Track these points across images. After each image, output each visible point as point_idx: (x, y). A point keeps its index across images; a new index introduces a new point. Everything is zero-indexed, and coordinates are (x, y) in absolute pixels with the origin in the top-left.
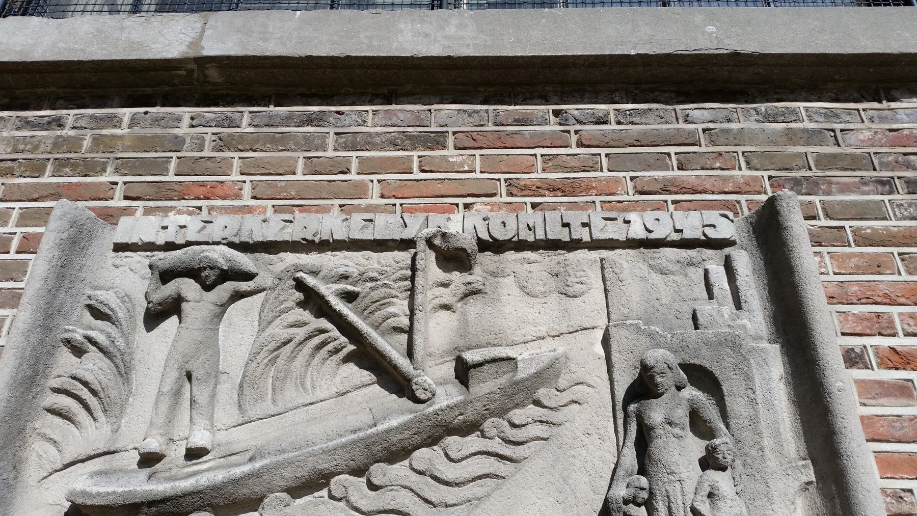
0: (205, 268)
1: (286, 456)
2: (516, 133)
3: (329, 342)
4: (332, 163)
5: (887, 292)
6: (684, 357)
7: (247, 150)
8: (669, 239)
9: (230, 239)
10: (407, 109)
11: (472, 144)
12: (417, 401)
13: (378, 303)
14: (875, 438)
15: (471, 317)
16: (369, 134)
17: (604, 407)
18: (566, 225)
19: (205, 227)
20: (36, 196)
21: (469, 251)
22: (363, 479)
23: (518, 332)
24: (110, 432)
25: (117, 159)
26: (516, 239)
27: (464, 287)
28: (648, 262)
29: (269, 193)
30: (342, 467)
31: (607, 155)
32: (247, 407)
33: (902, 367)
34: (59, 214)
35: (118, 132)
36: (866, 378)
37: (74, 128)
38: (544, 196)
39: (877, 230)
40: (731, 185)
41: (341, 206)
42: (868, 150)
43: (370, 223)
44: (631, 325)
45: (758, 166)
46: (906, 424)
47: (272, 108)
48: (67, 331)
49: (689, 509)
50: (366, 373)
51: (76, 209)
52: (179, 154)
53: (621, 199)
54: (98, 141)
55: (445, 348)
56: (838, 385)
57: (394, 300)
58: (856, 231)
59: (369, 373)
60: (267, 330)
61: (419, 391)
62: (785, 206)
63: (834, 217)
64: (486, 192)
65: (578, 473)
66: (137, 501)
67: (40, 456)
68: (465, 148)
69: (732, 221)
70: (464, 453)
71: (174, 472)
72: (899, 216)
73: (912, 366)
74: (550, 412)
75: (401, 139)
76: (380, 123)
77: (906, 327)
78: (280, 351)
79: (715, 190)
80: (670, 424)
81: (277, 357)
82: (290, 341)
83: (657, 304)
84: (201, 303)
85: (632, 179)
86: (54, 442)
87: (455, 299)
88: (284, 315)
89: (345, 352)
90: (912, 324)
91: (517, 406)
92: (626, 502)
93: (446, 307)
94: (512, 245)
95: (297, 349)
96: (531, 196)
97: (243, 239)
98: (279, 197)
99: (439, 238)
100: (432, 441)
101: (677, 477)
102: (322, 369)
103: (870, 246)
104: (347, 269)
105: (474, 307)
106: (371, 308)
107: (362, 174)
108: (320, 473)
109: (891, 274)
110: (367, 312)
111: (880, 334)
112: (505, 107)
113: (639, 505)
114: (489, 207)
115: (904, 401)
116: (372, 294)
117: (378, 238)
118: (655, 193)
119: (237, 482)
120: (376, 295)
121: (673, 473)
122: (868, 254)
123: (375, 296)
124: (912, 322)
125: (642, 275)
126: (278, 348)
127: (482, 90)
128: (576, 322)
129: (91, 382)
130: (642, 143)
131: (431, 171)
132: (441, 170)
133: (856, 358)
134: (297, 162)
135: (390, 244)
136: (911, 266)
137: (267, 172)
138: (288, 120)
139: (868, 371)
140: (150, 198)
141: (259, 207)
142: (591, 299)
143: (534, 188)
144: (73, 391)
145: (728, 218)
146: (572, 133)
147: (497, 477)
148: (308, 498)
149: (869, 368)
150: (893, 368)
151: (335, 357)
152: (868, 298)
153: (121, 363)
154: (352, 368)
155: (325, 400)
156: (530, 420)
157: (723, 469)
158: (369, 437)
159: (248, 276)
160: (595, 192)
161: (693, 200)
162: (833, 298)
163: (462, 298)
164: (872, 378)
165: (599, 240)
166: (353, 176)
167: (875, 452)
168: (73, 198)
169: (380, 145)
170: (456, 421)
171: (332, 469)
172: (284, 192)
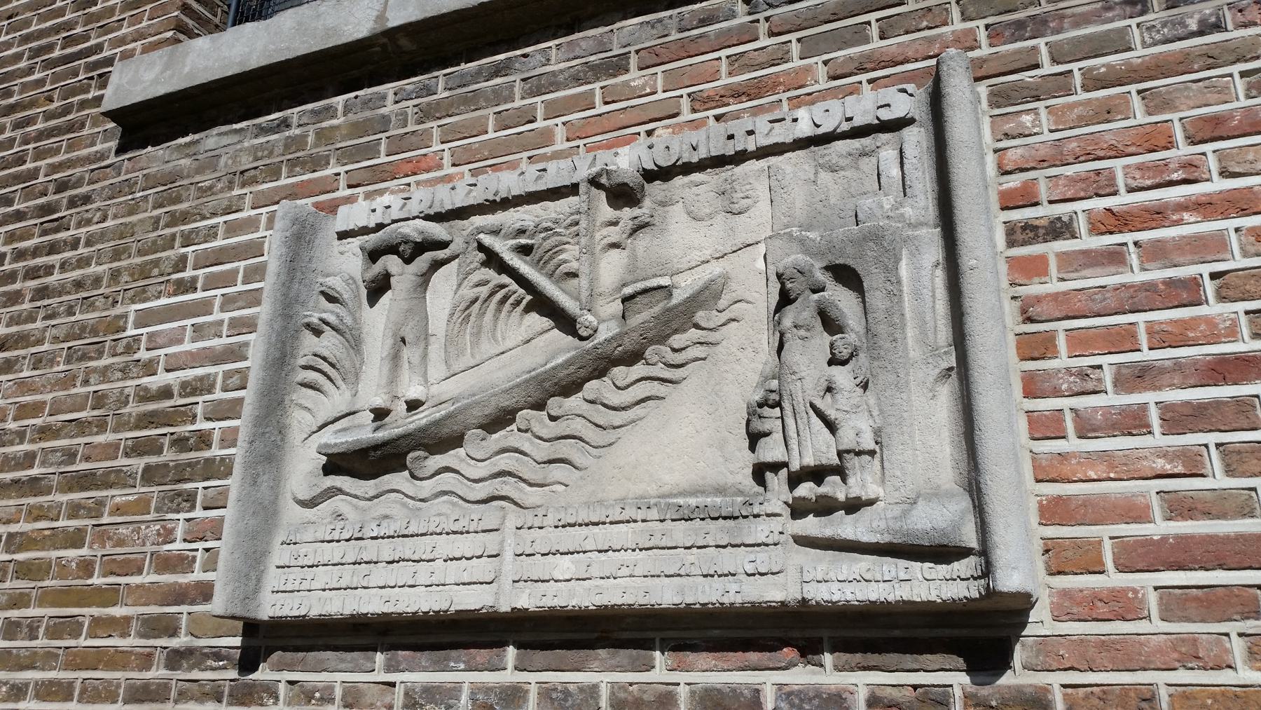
0: (400, 244)
2: (701, 36)
3: (510, 296)
4: (519, 114)
5: (1114, 142)
6: (830, 258)
7: (444, 117)
8: (839, 131)
9: (426, 212)
12: (582, 339)
13: (551, 252)
14: (1070, 314)
15: (640, 252)
16: (553, 73)
17: (760, 320)
18: (731, 137)
19: (405, 204)
21: (631, 185)
23: (684, 260)
25: (338, 149)
27: (632, 223)
28: (818, 161)
31: (799, 40)
33: (1117, 230)
35: (335, 122)
36: (1070, 249)
38: (728, 105)
39: (1113, 66)
40: (938, 46)
41: (530, 158)
44: (784, 234)
45: (974, 15)
47: (463, 66)
49: (808, 405)
50: (545, 319)
51: (296, 207)
52: (387, 134)
53: (810, 91)
54: (320, 134)
56: (970, 263)
57: (566, 246)
58: (1085, 73)
62: (945, 69)
63: (1061, 60)
65: (731, 386)
69: (911, 95)
70: (629, 380)
71: (400, 422)
72: (1149, 41)
73: (1130, 227)
74: (709, 332)
75: (583, 71)
77: (1130, 181)
78: (471, 309)
79: (918, 56)
80: (795, 327)
81: (469, 315)
82: (476, 300)
83: (819, 206)
85: (825, 63)
87: (625, 236)
89: (524, 302)
90: (1137, 177)
91: (676, 331)
92: (760, 405)
93: (615, 245)
94: (679, 170)
95: (484, 306)
96: (714, 108)
99: (605, 176)
100: (600, 373)
101: (798, 376)
103: (1103, 88)
104: (523, 223)
105: (643, 241)
106: (546, 258)
108: (505, 410)
109: (1123, 119)
110: (542, 262)
112: (690, 7)
113: (772, 407)
114: (670, 130)
115: (1113, 269)
118: (850, 75)
119: (437, 423)
121: (794, 373)
122: (1097, 99)
124: (1138, 174)
125: (806, 178)
126: (468, 308)
128: (744, 238)
130: (839, 16)
131: (614, 102)
133: (1062, 228)
134: (488, 119)
137: (462, 136)
138: (477, 76)
139: (1076, 240)
141: (457, 174)
142: (757, 213)
143: (717, 98)
145: (907, 92)
146: (762, 20)
147: (658, 398)
149: (1077, 238)
150: (1106, 232)
151: (518, 309)
152: (1089, 154)
156: (689, 343)
157: (844, 363)
159: (443, 245)
160: (782, 88)
161: (891, 75)
162: (1044, 161)
163: (631, 235)
164: (1077, 248)
165: (763, 148)
166: (540, 124)
167: (1066, 330)
169: (563, 83)
170: (616, 352)
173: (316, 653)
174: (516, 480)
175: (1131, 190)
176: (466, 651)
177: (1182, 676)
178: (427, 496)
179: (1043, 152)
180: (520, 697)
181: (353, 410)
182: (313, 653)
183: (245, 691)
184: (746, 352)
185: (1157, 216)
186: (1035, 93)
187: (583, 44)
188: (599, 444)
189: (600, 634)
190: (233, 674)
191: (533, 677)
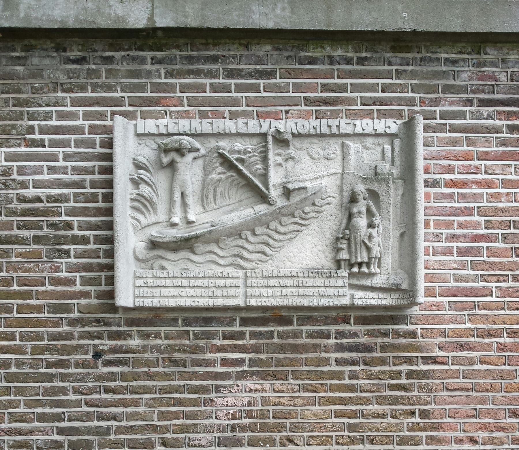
12: (271, 205)
15: (289, 169)
26: (307, 133)
42: (466, 83)
46: (448, 209)
70: (287, 223)
77: (459, 170)
83: (362, 164)
105: (290, 164)
111: (449, 173)
124: (462, 168)
136: (469, 143)
147: (298, 231)
175: (459, 173)
177: (452, 326)
179: (434, 154)
184: (333, 217)
185: (465, 184)
186: (433, 130)
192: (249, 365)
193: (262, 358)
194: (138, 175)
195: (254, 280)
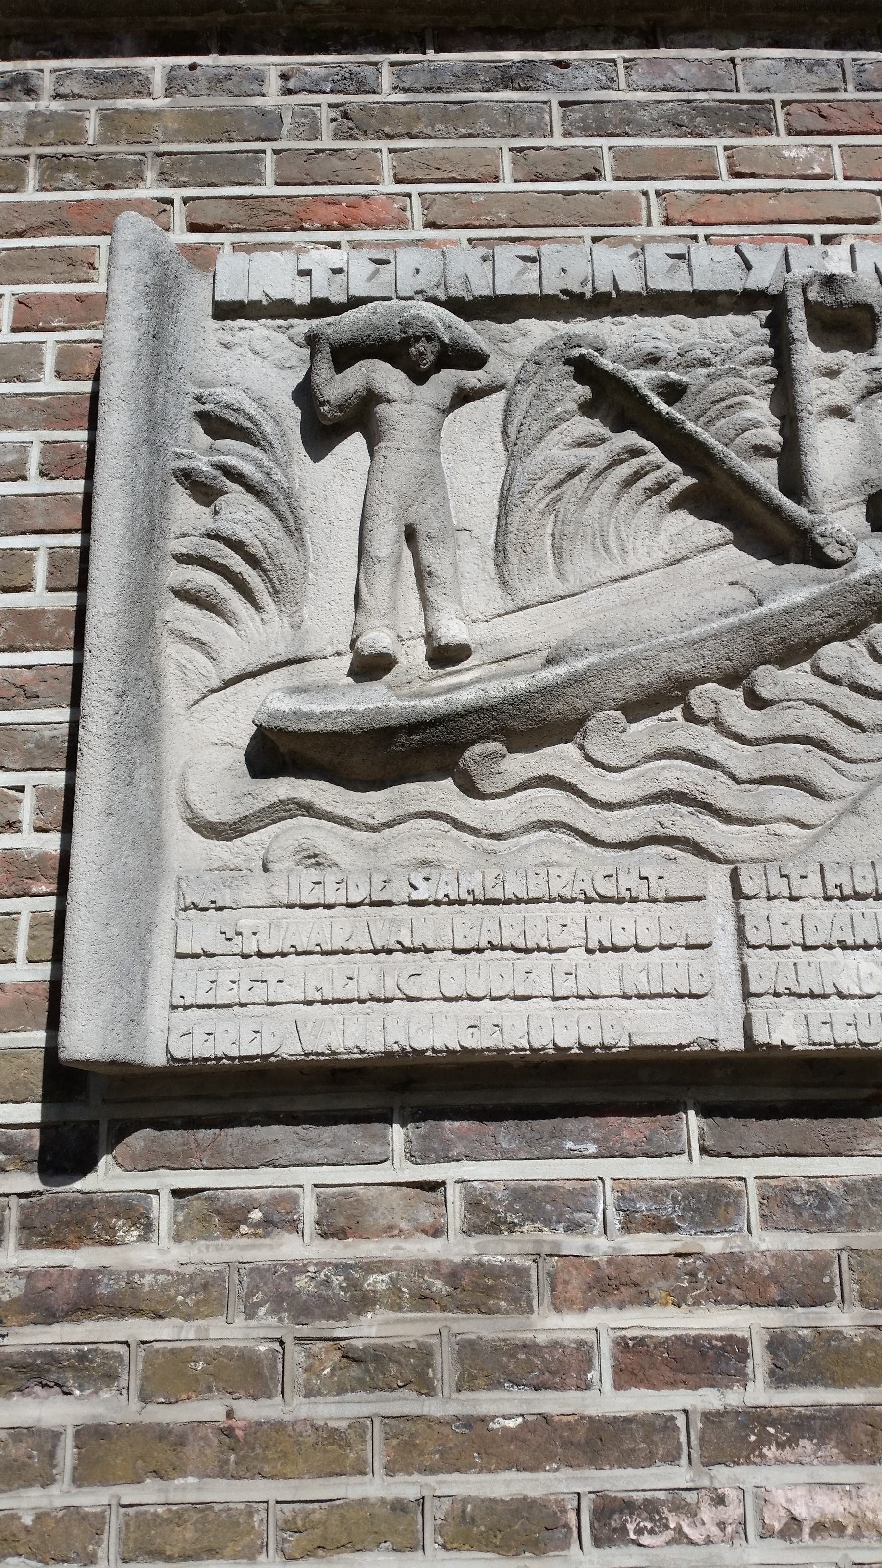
0: (417, 339)
1: (620, 651)
3: (647, 473)
4: (566, 159)
7: (401, 136)
9: (430, 293)
10: (690, 58)
11: (821, 124)
13: (723, 404)
16: (626, 104)
19: (377, 272)
20: (20, 226)
22: (739, 693)
24: (288, 629)
25: (159, 155)
27: (868, 377)
29: (457, 215)
30: (712, 670)
32: (515, 582)
34: (131, 237)
35: (146, 103)
37: (57, 96)
43: (680, 262)
47: (431, 55)
48: (179, 456)
50: (712, 525)
52: (277, 145)
54: (110, 120)
55: (848, 481)
57: (748, 398)
59: (718, 525)
60: (536, 452)
61: (830, 546)
64: (860, 215)
66: (393, 723)
67: (181, 667)
68: (809, 133)
71: (416, 686)
76: (642, 83)
78: (564, 488)
81: (558, 499)
82: (580, 470)
84: (414, 405)
86: (201, 645)
87: (852, 398)
88: (564, 426)
89: (675, 489)
93: (840, 412)
95: (593, 485)
97: (453, 292)
98: (477, 223)
99: (816, 286)
102: (634, 521)
104: (656, 343)
106: (712, 413)
107: (625, 179)
108: (678, 679)
116: (711, 387)
117: (703, 287)
119: (550, 691)
120: (719, 387)
123: (718, 391)
126: (561, 483)
127: (826, 21)
129: (248, 542)
131: (753, 176)
132: (771, 173)
135: (721, 300)
137: (446, 175)
138: (469, 73)
140: (240, 226)
144: (217, 559)
148: (649, 722)
151: (655, 500)
153: (288, 513)
154: (684, 519)
155: (647, 571)
158: (757, 620)
168: (94, 230)
169: (649, 125)
171: (696, 672)
172: (486, 214)
173: (245, 1129)
174: (691, 809)
176: (597, 1120)
178: (509, 828)
180: (728, 1204)
181: (301, 654)
182: (237, 1131)
183: (66, 1217)
187: (681, 70)
188: (861, 756)
189: (875, 1091)
190: (30, 1182)
191: (749, 1168)
192: (772, 1373)
193: (837, 1334)
194: (215, 458)
195: (782, 909)
